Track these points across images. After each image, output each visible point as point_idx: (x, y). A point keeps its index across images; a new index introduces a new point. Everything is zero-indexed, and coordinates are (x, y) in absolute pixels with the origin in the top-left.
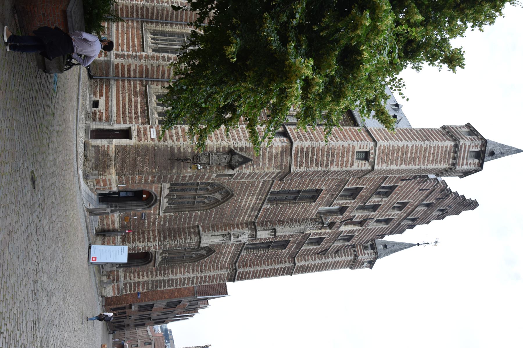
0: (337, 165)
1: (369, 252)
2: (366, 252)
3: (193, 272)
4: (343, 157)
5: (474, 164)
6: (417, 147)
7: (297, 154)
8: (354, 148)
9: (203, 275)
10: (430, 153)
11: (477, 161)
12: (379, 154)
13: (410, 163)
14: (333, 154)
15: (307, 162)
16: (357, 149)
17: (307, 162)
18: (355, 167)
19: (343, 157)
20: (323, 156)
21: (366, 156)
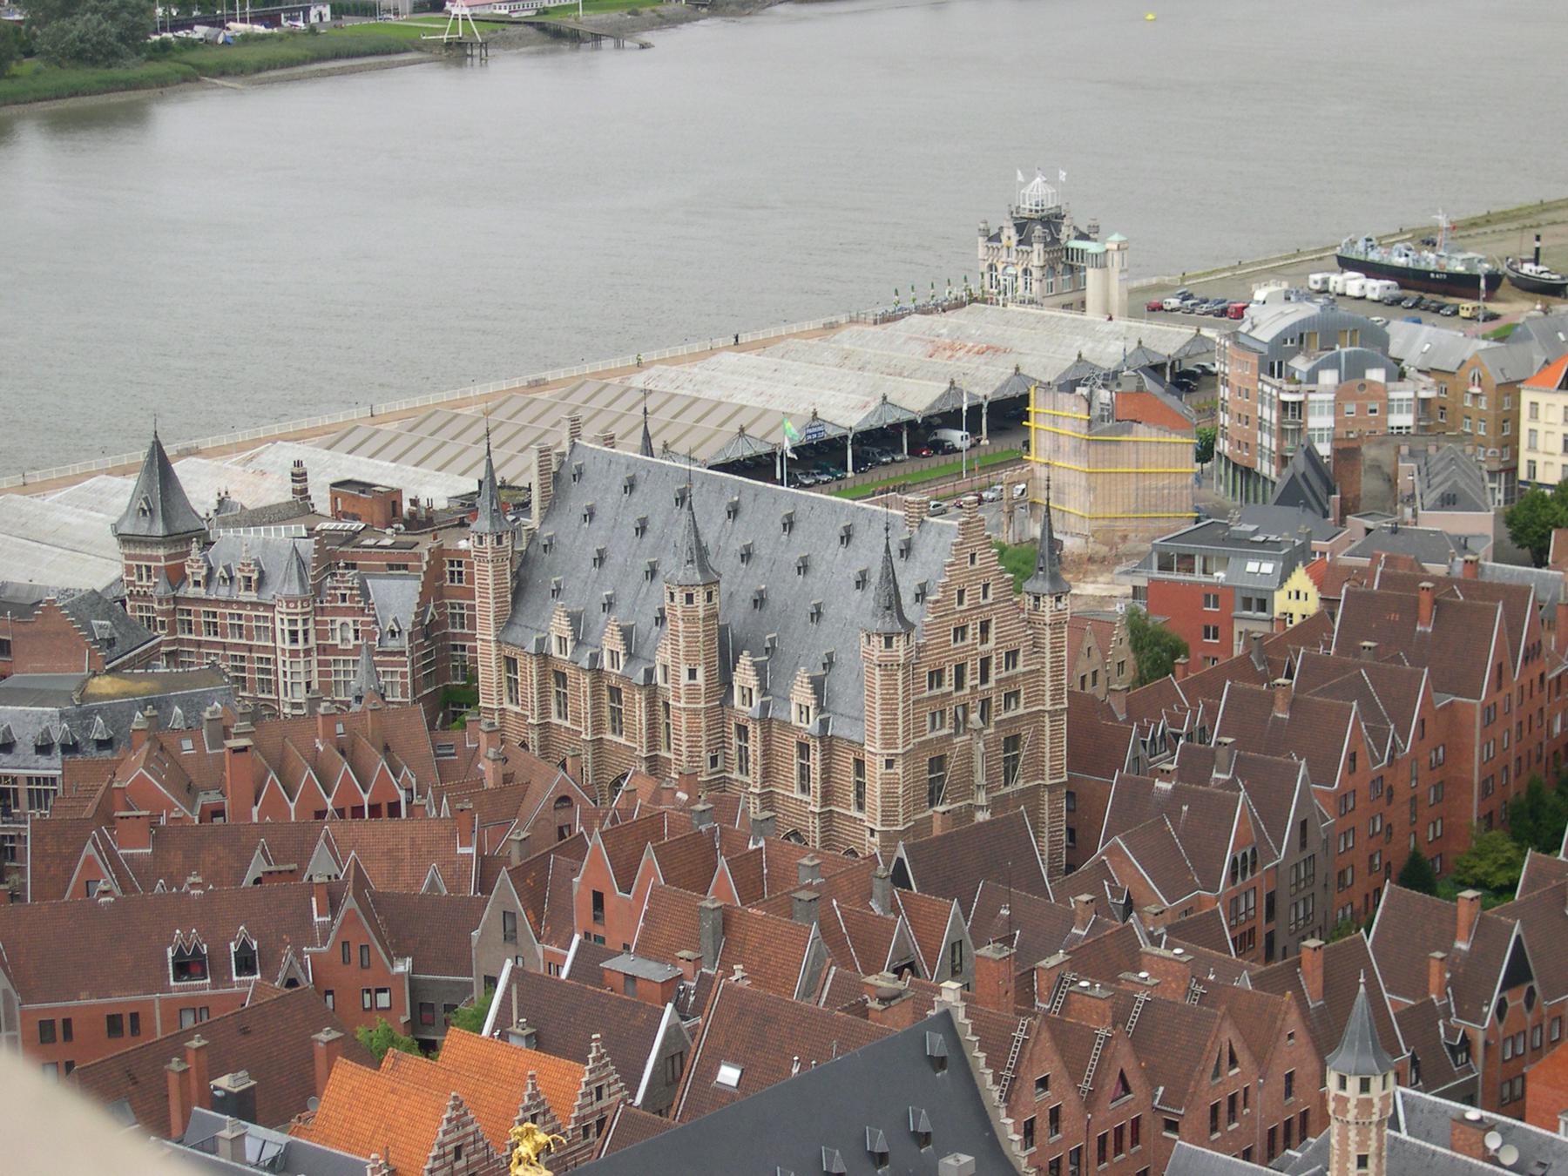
0: (897, 788)
1: (1042, 604)
2: (1041, 609)
3: (1043, 832)
4: (890, 783)
5: (898, 641)
6: (882, 709)
7: (888, 825)
8: (882, 774)
9: (1047, 821)
10: (887, 694)
11: (895, 639)
12: (888, 749)
13: (896, 714)
14: (888, 793)
15: (894, 816)
16: (884, 770)
17: (894, 816)
18: (900, 771)
19: (890, 783)
20: (889, 802)
21: (889, 764)
